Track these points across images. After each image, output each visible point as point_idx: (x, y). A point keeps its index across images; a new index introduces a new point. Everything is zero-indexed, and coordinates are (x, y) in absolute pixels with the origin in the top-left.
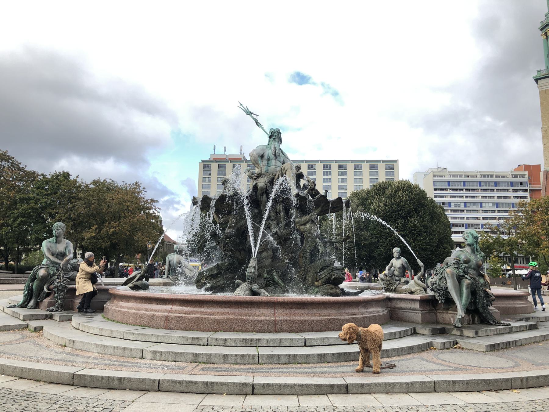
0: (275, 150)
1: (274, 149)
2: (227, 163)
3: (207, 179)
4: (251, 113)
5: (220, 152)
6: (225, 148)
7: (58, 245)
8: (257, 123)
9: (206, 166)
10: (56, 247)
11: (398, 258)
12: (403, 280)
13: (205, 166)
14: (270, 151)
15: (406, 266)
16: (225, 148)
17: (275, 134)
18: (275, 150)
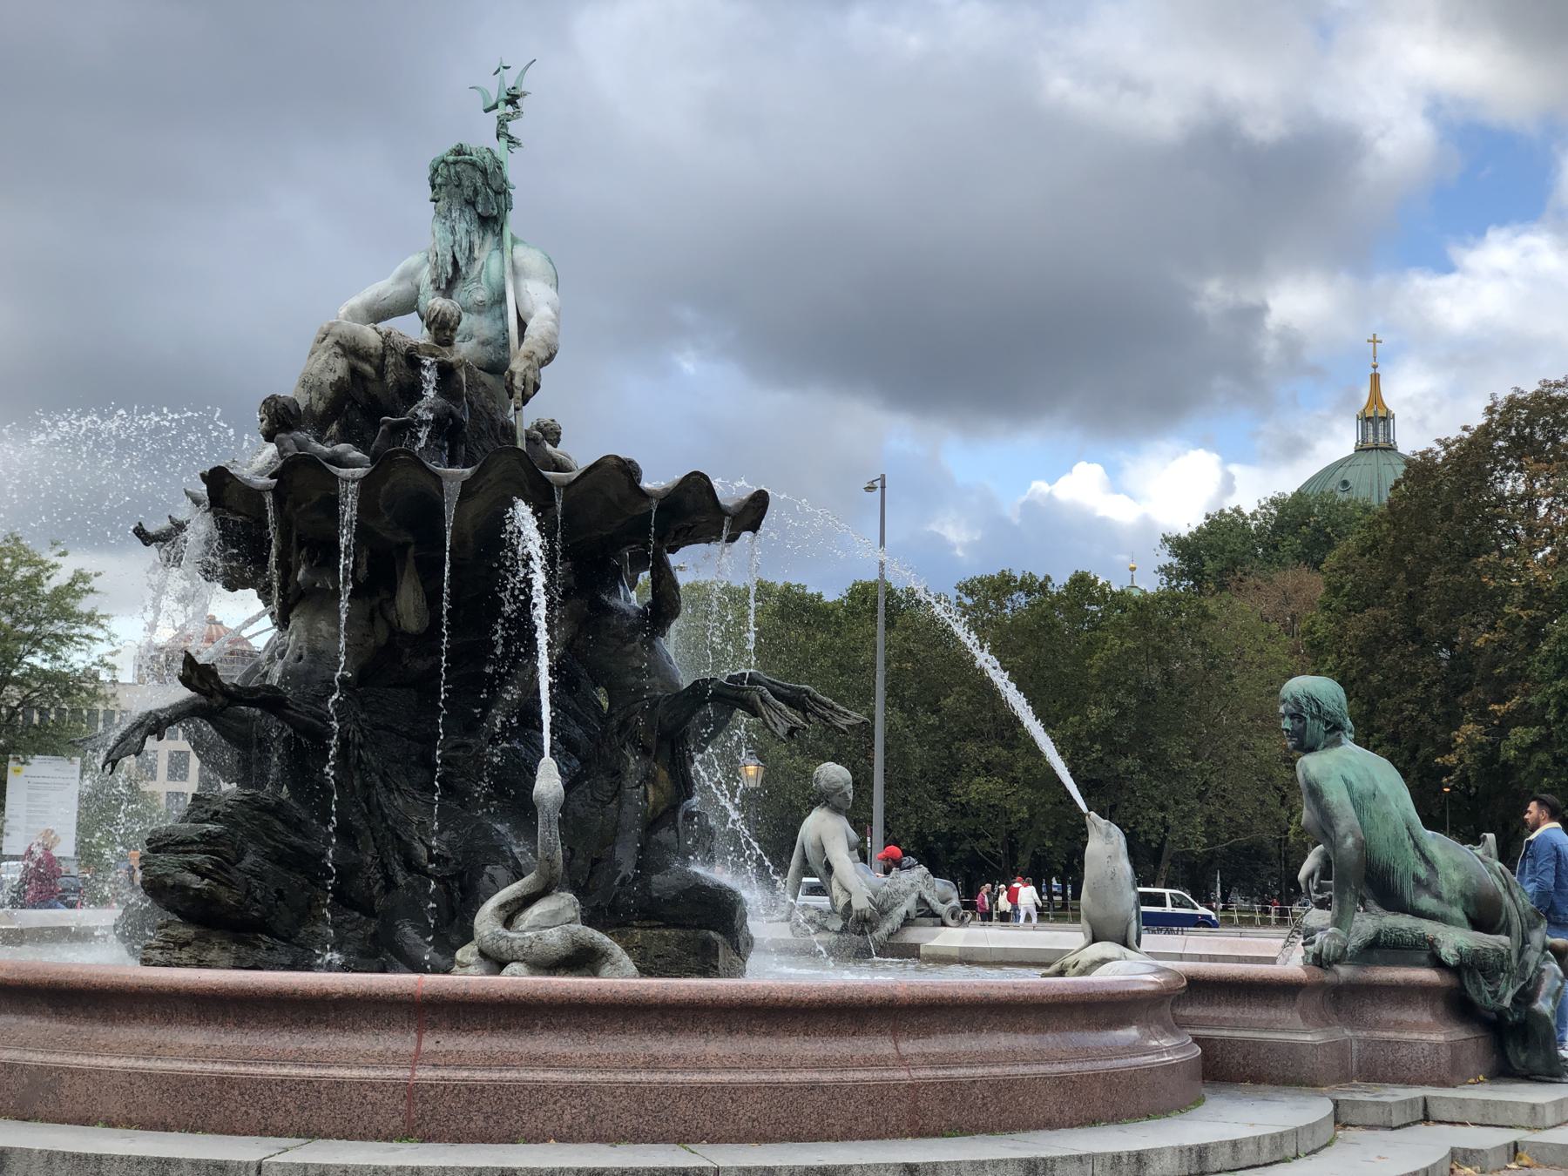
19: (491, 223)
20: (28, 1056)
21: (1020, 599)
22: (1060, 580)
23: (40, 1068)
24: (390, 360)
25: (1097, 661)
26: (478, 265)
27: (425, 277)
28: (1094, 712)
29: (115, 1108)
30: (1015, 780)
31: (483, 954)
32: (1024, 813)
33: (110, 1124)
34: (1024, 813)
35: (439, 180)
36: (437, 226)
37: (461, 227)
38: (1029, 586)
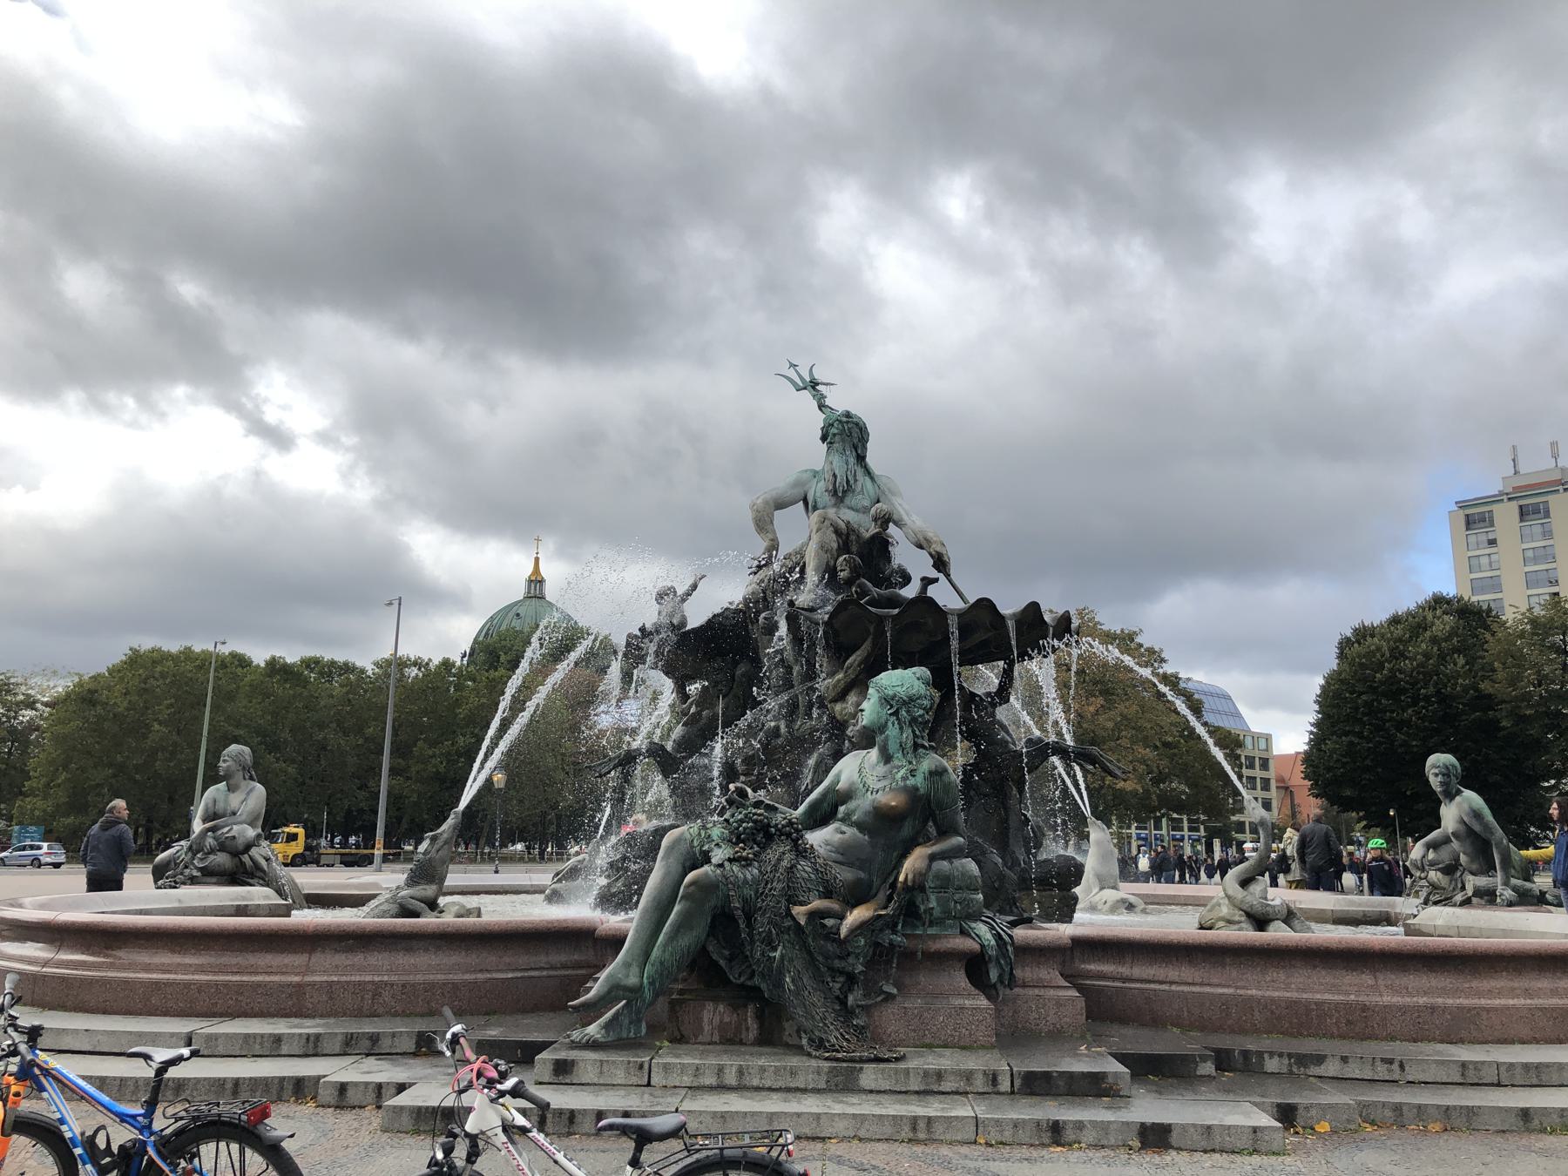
0: (835, 476)
1: (829, 476)
2: (1550, 498)
3: (1484, 561)
4: (814, 384)
5: (1537, 465)
6: (1554, 445)
7: (232, 796)
8: (821, 407)
9: (1475, 517)
10: (226, 801)
11: (1451, 795)
12: (1472, 882)
13: (1470, 523)
14: (822, 484)
15: (1477, 827)
16: (1554, 445)
17: (834, 430)
18: (835, 476)
19: (861, 459)
20: (1440, 1000)
21: (414, 672)
22: (436, 661)
23: (1460, 1008)
24: (853, 537)
25: (462, 712)
26: (859, 484)
27: (818, 490)
28: (461, 740)
29: (1525, 1032)
30: (408, 778)
31: (1249, 915)
32: (414, 798)
33: (1523, 1042)
34: (414, 798)
35: (834, 430)
36: (837, 461)
37: (852, 460)
38: (417, 663)
